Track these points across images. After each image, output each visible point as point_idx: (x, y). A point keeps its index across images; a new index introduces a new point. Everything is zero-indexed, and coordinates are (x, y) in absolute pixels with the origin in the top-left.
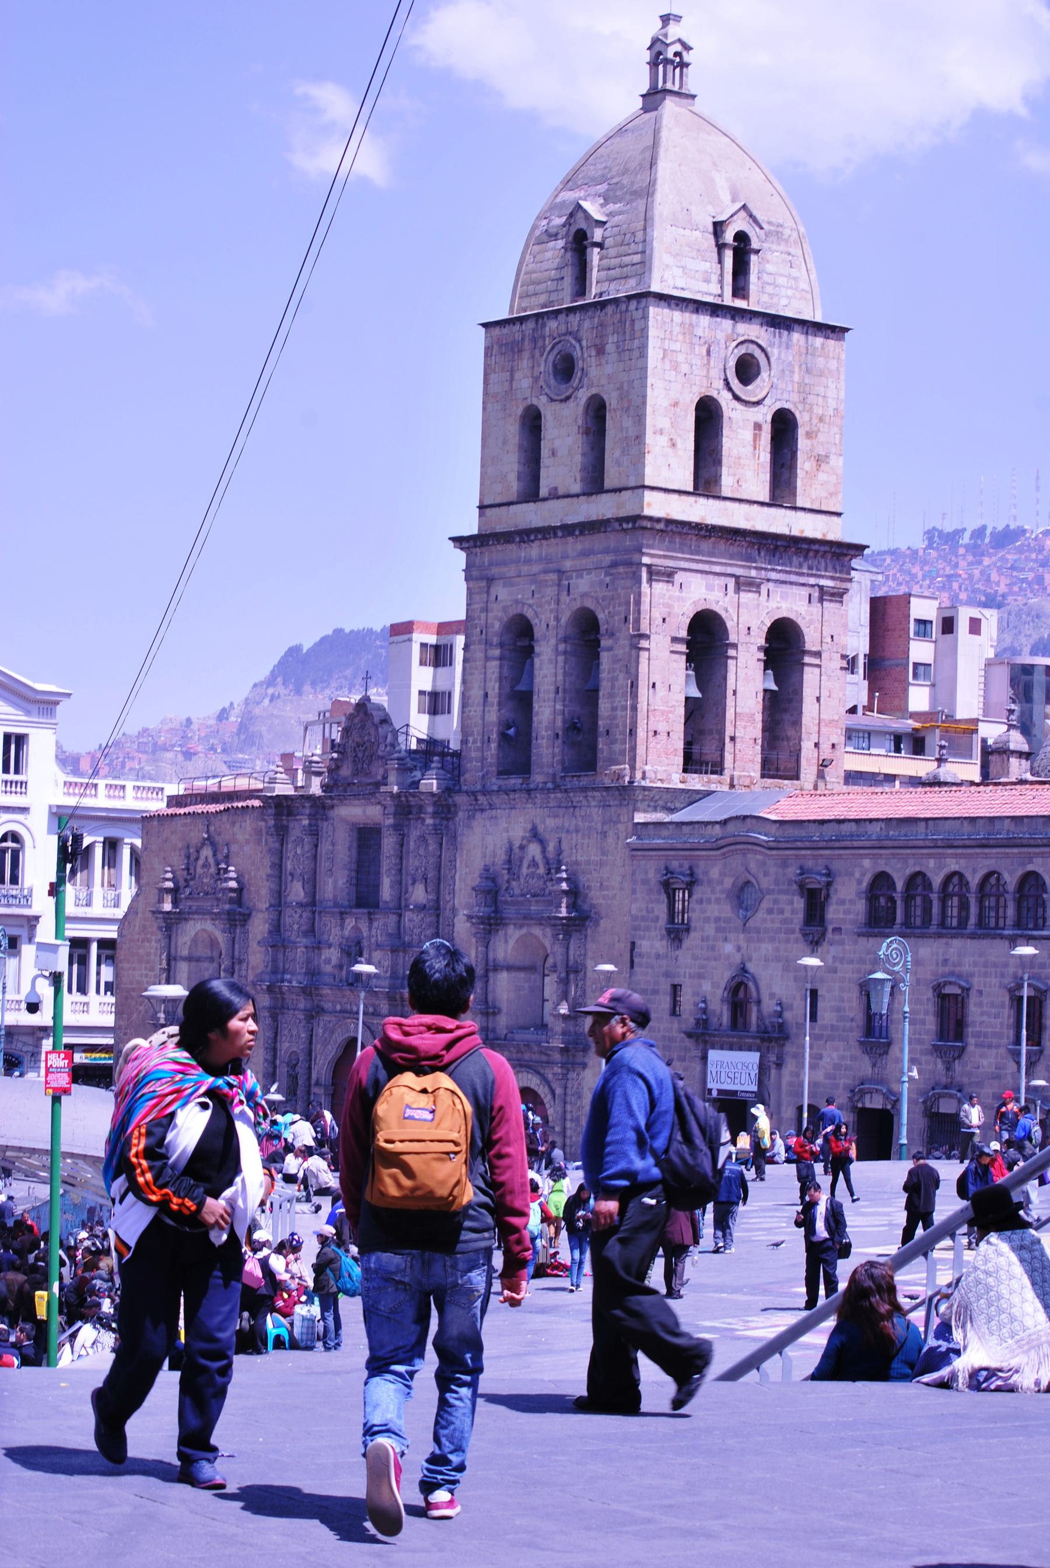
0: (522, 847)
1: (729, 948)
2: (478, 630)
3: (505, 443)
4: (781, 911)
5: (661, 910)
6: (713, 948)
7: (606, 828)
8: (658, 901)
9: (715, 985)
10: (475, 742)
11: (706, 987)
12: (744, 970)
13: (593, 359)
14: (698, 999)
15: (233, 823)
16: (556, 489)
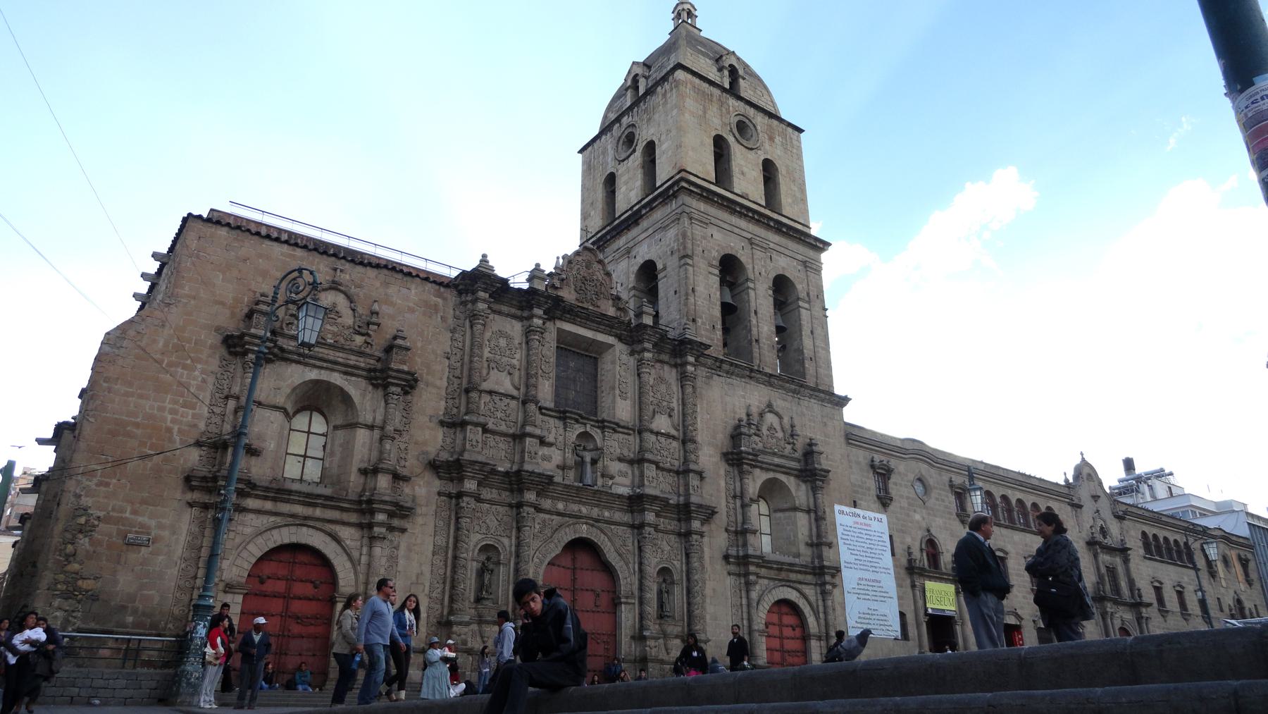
0: (761, 415)
1: (917, 517)
2: (701, 249)
3: (702, 144)
4: (943, 501)
5: (871, 483)
6: (908, 515)
7: (825, 420)
8: (868, 478)
9: (913, 539)
10: (703, 323)
11: (908, 540)
12: (928, 531)
13: (767, 141)
14: (906, 547)
15: (386, 284)
16: (747, 194)
